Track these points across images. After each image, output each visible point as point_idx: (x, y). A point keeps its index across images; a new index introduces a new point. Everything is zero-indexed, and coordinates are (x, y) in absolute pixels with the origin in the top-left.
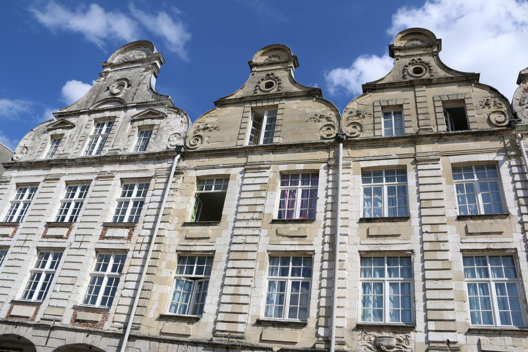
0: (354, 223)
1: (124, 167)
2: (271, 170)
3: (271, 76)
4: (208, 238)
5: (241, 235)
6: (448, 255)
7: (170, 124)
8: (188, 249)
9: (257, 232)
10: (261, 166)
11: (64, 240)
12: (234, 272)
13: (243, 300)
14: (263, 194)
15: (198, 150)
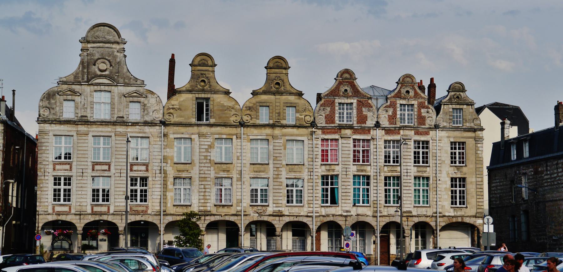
0: (248, 165)
1: (130, 129)
2: (211, 137)
3: (204, 76)
4: (188, 171)
5: (203, 170)
6: (281, 180)
7: (150, 102)
8: (179, 176)
9: (209, 169)
10: (207, 136)
11: (109, 172)
12: (202, 186)
13: (208, 197)
14: (209, 150)
15: (172, 123)
